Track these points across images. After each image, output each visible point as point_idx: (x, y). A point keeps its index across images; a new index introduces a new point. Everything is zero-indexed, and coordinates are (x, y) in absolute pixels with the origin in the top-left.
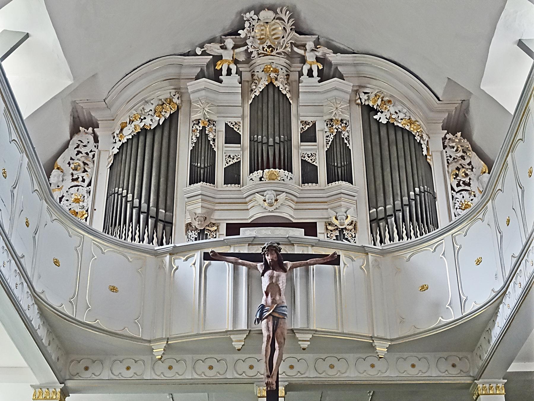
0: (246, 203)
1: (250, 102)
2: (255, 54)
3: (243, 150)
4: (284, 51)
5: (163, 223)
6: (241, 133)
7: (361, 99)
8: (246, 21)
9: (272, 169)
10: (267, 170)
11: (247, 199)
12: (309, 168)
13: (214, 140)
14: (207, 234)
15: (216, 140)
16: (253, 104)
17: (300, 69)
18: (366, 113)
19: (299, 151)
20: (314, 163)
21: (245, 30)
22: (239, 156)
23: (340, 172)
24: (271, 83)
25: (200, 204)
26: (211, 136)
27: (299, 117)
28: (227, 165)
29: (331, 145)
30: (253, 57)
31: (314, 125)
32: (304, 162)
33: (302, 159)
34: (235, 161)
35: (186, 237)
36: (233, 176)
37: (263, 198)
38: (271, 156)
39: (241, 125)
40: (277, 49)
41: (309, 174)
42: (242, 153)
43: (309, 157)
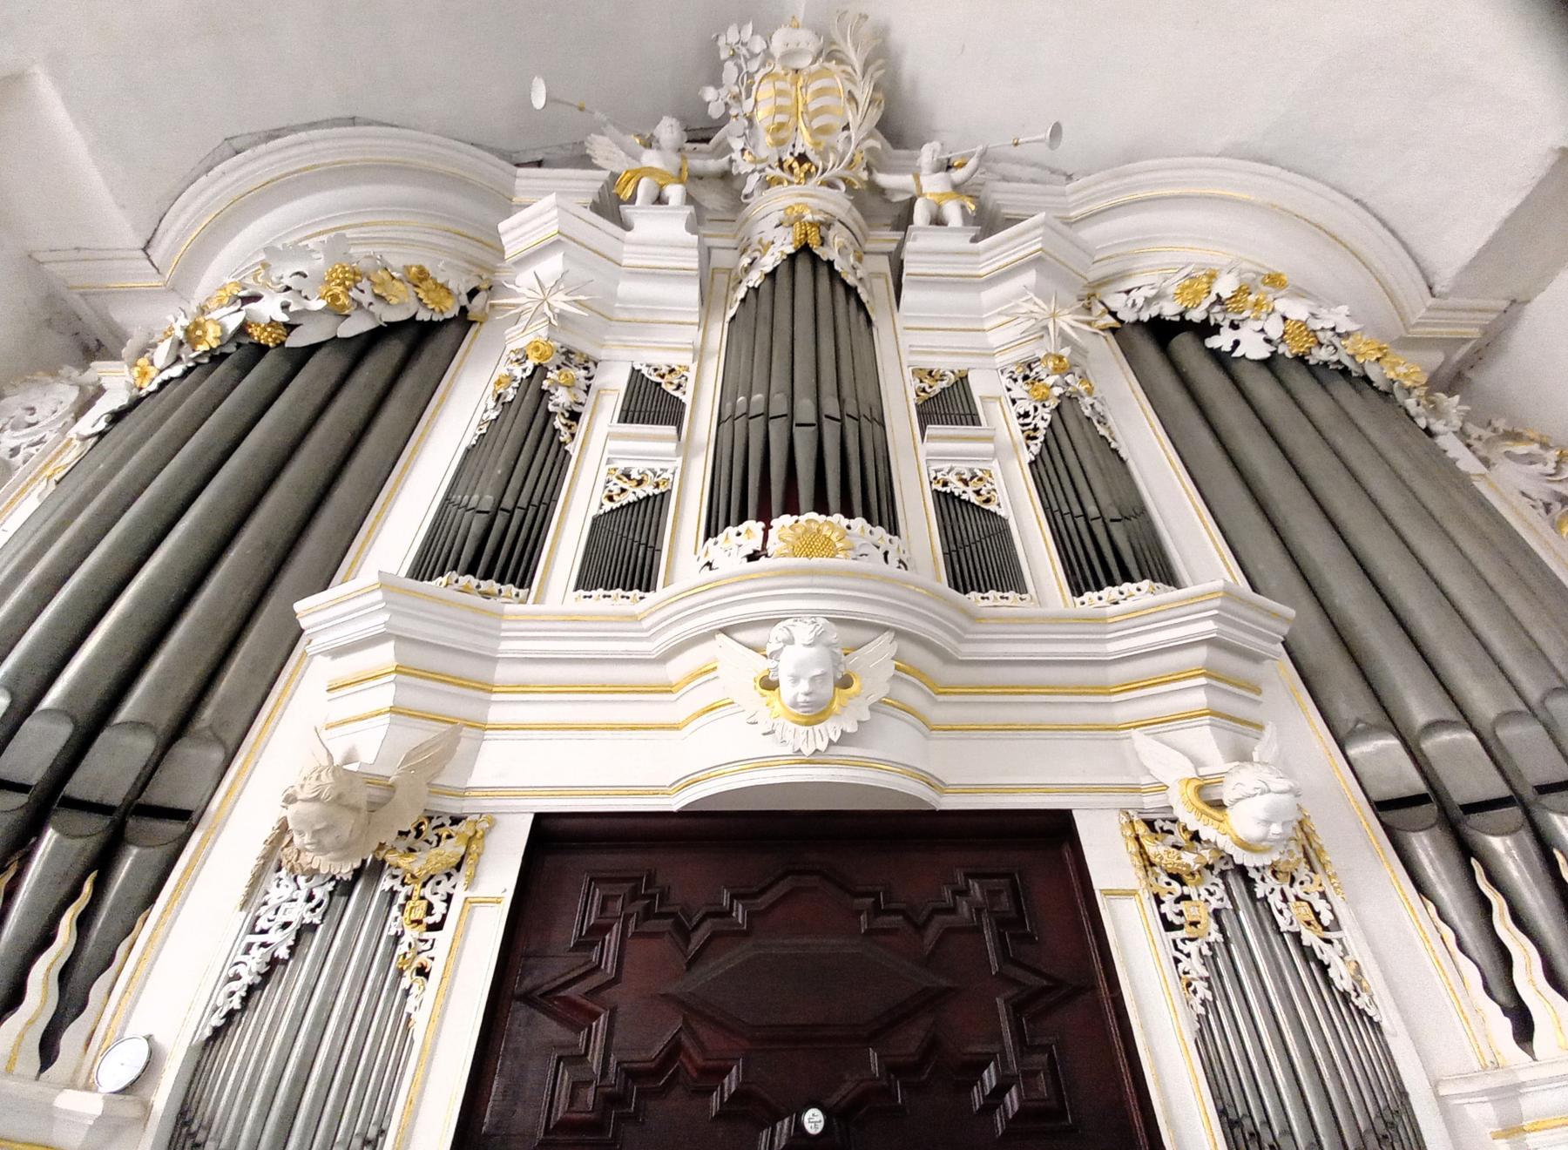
0: (667, 689)
1: (731, 313)
2: (753, 181)
4: (846, 174)
5: (99, 823)
6: (687, 399)
7: (1113, 314)
9: (814, 515)
10: (787, 520)
11: (675, 669)
13: (575, 416)
14: (393, 893)
15: (584, 420)
17: (892, 247)
18: (1148, 350)
19: (919, 462)
20: (992, 507)
21: (723, 92)
22: (665, 475)
23: (1114, 548)
24: (805, 249)
25: (384, 695)
26: (561, 398)
27: (912, 343)
28: (608, 506)
29: (1045, 441)
30: (746, 197)
31: (963, 380)
32: (946, 502)
34: (649, 490)
35: (238, 920)
36: (626, 554)
37: (761, 665)
38: (806, 456)
39: (691, 375)
40: (824, 171)
41: (976, 553)
42: (682, 464)
43: (966, 483)
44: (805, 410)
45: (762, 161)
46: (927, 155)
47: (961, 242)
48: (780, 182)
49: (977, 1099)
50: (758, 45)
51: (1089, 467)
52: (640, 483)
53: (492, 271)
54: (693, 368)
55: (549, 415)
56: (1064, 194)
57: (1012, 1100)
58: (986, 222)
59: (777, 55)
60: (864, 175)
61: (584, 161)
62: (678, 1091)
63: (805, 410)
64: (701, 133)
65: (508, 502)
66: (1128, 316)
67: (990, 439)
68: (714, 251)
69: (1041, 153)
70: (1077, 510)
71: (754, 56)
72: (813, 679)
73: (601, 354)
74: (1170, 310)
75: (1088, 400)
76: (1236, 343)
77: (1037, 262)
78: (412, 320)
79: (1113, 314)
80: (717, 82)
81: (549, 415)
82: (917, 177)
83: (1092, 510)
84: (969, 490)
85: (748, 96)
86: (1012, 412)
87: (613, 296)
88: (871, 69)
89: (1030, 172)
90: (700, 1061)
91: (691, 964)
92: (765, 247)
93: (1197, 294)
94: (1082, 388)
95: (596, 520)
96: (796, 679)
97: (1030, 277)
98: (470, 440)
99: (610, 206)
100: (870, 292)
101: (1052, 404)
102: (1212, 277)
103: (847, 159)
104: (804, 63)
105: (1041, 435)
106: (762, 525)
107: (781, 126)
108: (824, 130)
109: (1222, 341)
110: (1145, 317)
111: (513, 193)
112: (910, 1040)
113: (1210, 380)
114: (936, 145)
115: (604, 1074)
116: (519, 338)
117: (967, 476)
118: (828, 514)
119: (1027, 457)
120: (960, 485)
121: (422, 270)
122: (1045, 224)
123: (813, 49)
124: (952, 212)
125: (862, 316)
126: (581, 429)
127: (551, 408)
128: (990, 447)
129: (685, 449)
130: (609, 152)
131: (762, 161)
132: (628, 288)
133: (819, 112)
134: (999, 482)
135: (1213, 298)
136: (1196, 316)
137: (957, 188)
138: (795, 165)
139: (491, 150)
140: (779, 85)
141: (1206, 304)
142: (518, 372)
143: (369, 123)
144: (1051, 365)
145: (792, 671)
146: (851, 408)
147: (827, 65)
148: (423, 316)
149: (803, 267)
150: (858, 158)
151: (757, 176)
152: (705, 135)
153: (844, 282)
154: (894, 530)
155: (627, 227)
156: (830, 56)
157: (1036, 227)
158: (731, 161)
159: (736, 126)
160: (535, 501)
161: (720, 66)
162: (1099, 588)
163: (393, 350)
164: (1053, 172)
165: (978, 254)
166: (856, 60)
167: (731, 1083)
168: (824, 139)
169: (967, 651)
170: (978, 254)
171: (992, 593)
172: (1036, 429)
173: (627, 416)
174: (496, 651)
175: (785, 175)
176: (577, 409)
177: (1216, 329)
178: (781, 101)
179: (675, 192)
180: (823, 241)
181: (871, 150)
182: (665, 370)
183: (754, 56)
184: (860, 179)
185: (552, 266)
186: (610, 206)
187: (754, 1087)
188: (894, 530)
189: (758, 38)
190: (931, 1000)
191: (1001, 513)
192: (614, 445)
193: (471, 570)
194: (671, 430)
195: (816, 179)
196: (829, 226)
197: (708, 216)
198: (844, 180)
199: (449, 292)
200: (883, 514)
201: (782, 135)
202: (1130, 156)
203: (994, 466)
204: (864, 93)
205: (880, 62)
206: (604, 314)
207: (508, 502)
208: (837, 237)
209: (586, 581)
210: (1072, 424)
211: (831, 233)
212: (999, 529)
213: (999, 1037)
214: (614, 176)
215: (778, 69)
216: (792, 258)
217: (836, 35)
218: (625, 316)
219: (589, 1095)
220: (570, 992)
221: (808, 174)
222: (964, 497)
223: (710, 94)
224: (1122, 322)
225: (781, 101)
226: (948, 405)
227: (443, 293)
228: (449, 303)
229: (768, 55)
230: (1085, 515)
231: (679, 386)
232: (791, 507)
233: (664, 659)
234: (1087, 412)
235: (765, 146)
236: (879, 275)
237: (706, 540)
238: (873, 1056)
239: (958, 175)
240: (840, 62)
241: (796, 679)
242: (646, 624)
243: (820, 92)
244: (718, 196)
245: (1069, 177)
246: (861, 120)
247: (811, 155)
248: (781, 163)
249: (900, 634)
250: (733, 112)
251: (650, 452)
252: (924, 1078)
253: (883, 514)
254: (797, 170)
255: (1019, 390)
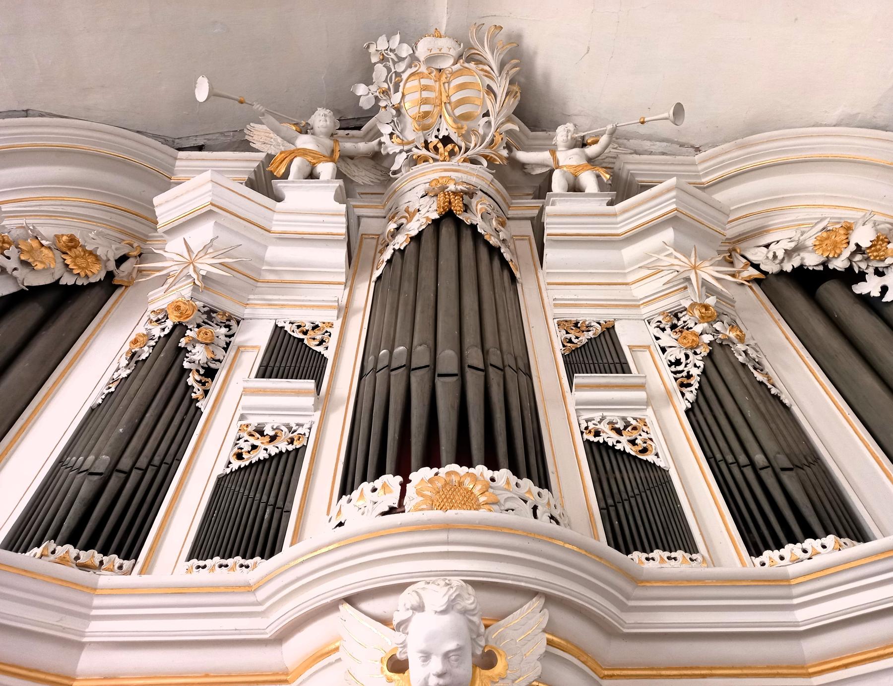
1: (377, 273)
2: (400, 160)
3: (323, 404)
4: (488, 152)
6: (329, 354)
7: (756, 266)
8: (375, 64)
9: (455, 467)
10: (426, 473)
12: (629, 479)
13: (210, 373)
15: (220, 377)
16: (386, 280)
17: (535, 212)
19: (568, 412)
20: (650, 457)
21: (373, 88)
22: (301, 431)
26: (199, 354)
27: (557, 296)
28: (236, 464)
29: (700, 389)
30: (395, 173)
31: (609, 331)
32: (599, 453)
33: (588, 443)
34: (283, 446)
36: (251, 517)
39: (335, 332)
40: (467, 150)
41: (637, 510)
43: (619, 432)
44: (448, 359)
45: (409, 143)
46: (562, 134)
47: (599, 205)
48: (426, 160)
50: (405, 51)
51: (749, 413)
52: (273, 439)
53: (144, 239)
54: (338, 324)
55: (184, 372)
56: (693, 164)
58: (621, 188)
59: (422, 59)
60: (505, 153)
61: (245, 145)
63: (448, 359)
64: (353, 120)
65: (125, 463)
66: (772, 268)
67: (641, 387)
68: (363, 220)
69: (667, 129)
70: (743, 459)
71: (401, 59)
72: (446, 656)
73: (247, 312)
74: (812, 260)
75: (741, 347)
76: (884, 289)
77: (673, 221)
78: (56, 284)
79: (756, 266)
80: (368, 82)
81: (184, 372)
82: (553, 153)
83: (759, 458)
84: (624, 439)
85: (396, 91)
86: (662, 360)
87: (262, 260)
88: (507, 67)
89: (659, 146)
92: (411, 215)
93: (835, 245)
94: (732, 335)
95: (221, 480)
96: (426, 656)
97: (668, 234)
98: (96, 398)
99: (264, 182)
100: (514, 253)
101: (704, 351)
102: (848, 229)
103: (488, 139)
104: (446, 64)
105: (695, 382)
106: (399, 479)
107: (426, 114)
108: (466, 117)
109: (870, 287)
110: (788, 268)
111: (172, 172)
113: (864, 325)
114: (570, 126)
116: (161, 299)
117: (620, 425)
118: (470, 465)
119: (683, 405)
120: (616, 437)
121: (72, 239)
122: (677, 187)
123: (454, 53)
124: (588, 180)
125: (506, 273)
126: (215, 387)
127: (186, 365)
128: (641, 395)
129: (323, 404)
130: (266, 138)
131: (409, 143)
132: (276, 253)
133: (461, 102)
134: (655, 432)
135: (852, 247)
136: (839, 264)
137: (591, 161)
138: (440, 145)
139: (155, 137)
140: (424, 82)
141: (846, 253)
142: (157, 332)
143: (41, 115)
144: (697, 313)
145: (423, 646)
146: (494, 359)
147: (466, 65)
148: (68, 280)
149: (447, 231)
150: (498, 138)
151: (404, 155)
152: (358, 123)
153: (487, 243)
154: (544, 482)
155: (279, 199)
156: (469, 60)
157: (669, 190)
158: (380, 143)
159: (386, 115)
160: (157, 460)
161: (371, 67)
162: (779, 546)
163: (32, 312)
164: (682, 145)
165: (615, 215)
166: (493, 61)
168: (466, 125)
169: (632, 621)
170: (615, 215)
171: (657, 553)
172: (689, 376)
173: (264, 372)
174: (83, 634)
175: (432, 154)
176: (213, 366)
177: (861, 277)
178: (425, 94)
179: (326, 169)
180: (466, 208)
181: (509, 132)
182: (308, 327)
183: (401, 59)
184: (500, 157)
185: (201, 234)
186: (264, 182)
188: (544, 482)
189: (405, 46)
191: (660, 463)
192: (248, 401)
193: (73, 540)
194: (310, 384)
195: (458, 158)
196: (471, 195)
197: (359, 190)
198: (485, 157)
199: (97, 258)
200: (531, 463)
201: (429, 121)
202: (753, 129)
203: (649, 414)
204: (501, 87)
205: (515, 61)
206: (249, 276)
207: (125, 463)
208: (479, 205)
209: (203, 548)
210: (726, 371)
211: (474, 201)
212: (659, 481)
214: (270, 157)
215: (423, 69)
216: (436, 223)
217: (474, 42)
218: (272, 277)
221: (452, 154)
222: (619, 447)
223: (361, 89)
224: (765, 273)
225: (425, 94)
226: (597, 354)
227: (91, 259)
228: (96, 268)
229: (413, 58)
230: (752, 464)
231: (322, 342)
232: (432, 460)
233: (280, 639)
234: (741, 359)
235: (411, 133)
236: (522, 238)
237: (340, 497)
239: (591, 150)
240: (479, 62)
241: (426, 656)
242: (261, 595)
243: (462, 87)
244: (366, 174)
245: (698, 150)
246: (499, 108)
247: (454, 137)
248: (426, 144)
249: (550, 600)
250: (382, 104)
251: (287, 405)
253: (531, 463)
254: (441, 150)
255: (667, 338)
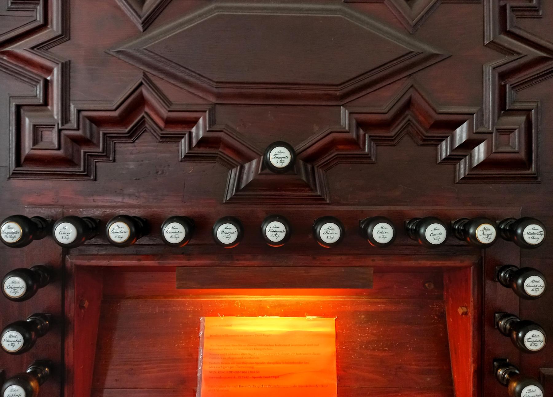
49: (444, 150)
57: (480, 153)
62: (146, 137)
90: (165, 113)
91: (148, 23)
112: (383, 102)
115: (65, 119)
167: (199, 131)
187: (222, 135)
190: (411, 65)
213: (479, 101)
219: (51, 137)
220: (20, 48)
238: (344, 114)
252: (393, 134)
